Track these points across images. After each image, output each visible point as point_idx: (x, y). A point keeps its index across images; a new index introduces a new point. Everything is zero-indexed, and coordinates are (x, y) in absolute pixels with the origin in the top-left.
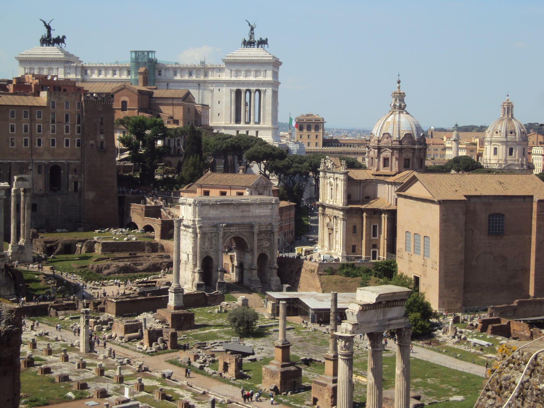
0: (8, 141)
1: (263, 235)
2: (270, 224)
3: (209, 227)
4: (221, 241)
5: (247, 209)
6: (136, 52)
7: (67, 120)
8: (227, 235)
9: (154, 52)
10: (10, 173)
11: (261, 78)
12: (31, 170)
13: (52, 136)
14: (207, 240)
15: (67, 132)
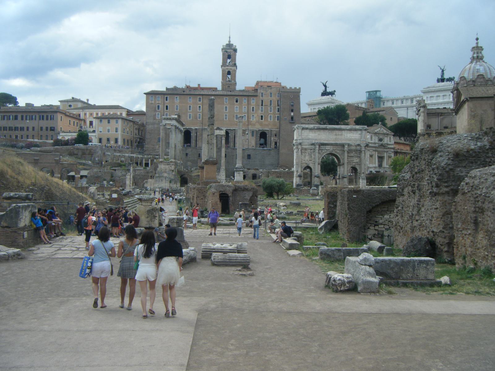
0: (234, 116)
1: (354, 153)
2: (359, 145)
3: (309, 145)
4: (317, 155)
5: (340, 134)
6: (369, 92)
7: (271, 104)
8: (323, 151)
9: (380, 91)
10: (235, 136)
11: (446, 100)
12: (247, 134)
13: (261, 113)
14: (307, 155)
15: (271, 111)
